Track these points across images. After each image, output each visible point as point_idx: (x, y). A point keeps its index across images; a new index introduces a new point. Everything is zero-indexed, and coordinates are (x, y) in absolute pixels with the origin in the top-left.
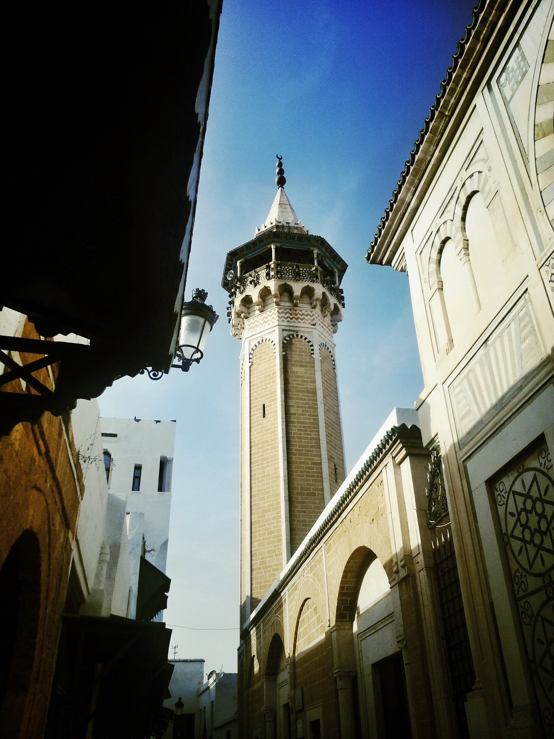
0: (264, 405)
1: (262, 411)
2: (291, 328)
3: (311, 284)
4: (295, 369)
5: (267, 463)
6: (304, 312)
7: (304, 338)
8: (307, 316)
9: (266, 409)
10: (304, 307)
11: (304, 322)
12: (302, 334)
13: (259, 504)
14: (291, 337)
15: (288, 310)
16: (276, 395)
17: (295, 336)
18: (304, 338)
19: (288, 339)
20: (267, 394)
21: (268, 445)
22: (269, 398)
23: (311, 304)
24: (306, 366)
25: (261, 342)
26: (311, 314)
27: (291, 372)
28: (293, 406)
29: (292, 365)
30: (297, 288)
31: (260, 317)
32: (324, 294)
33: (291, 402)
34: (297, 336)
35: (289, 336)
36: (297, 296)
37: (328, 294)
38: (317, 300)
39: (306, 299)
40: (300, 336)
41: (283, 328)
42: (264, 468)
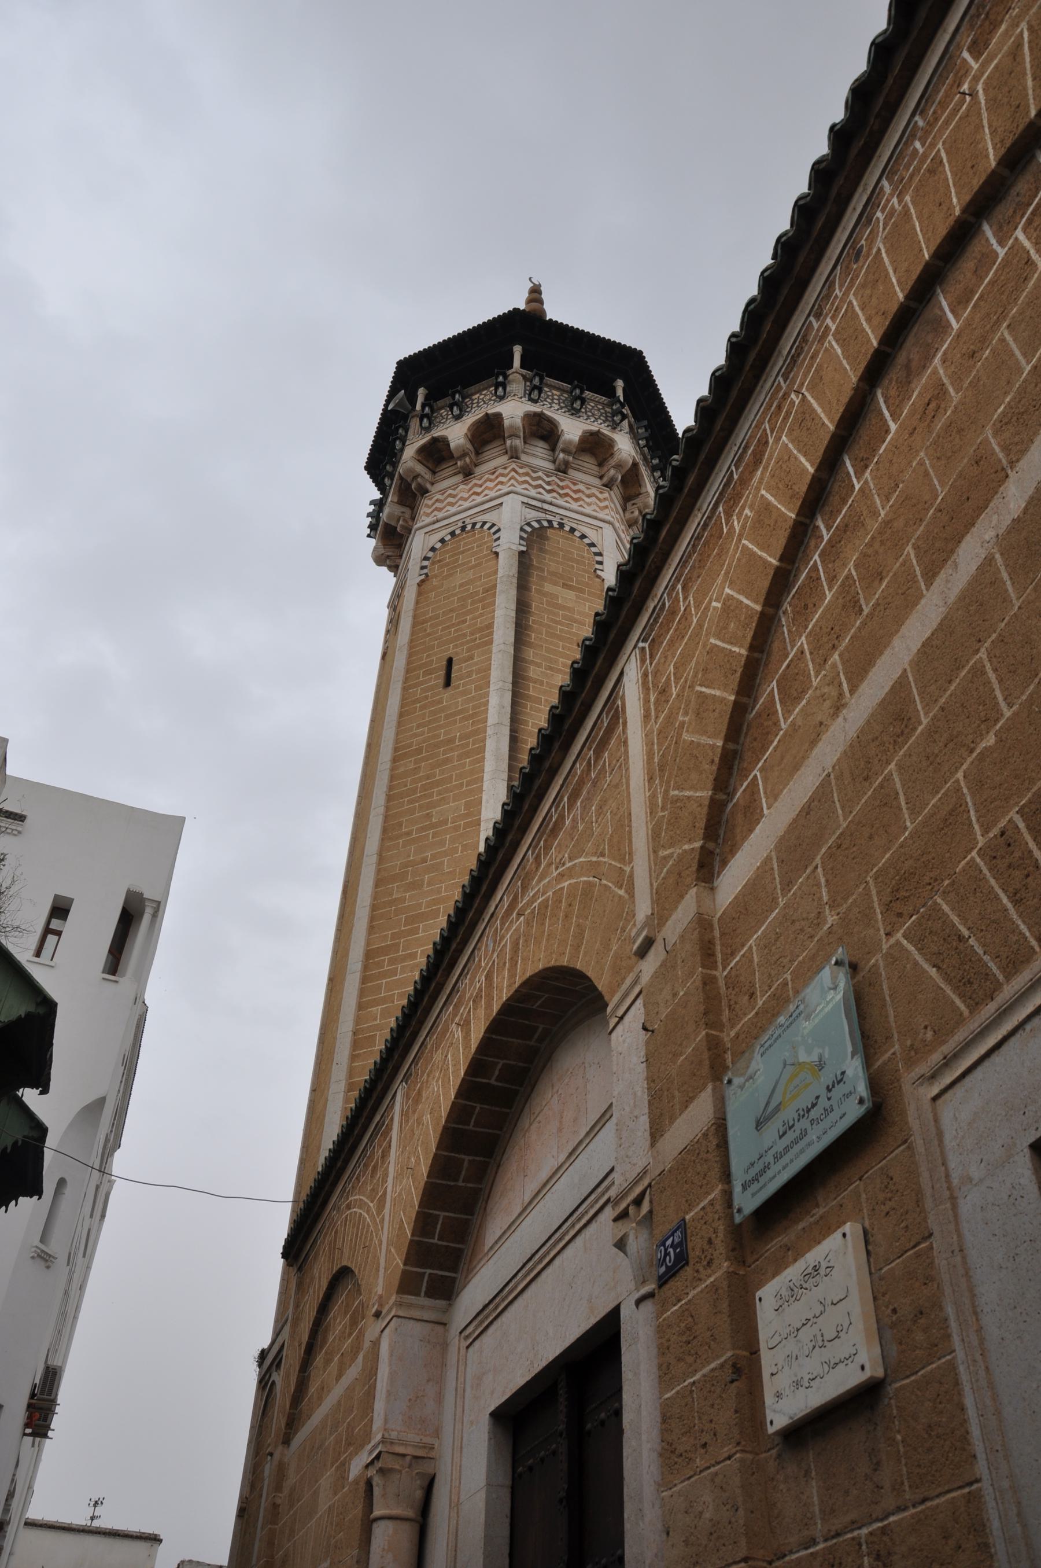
0: (450, 661)
1: (443, 673)
2: (546, 506)
3: (606, 431)
4: (548, 587)
5: (439, 793)
6: (581, 487)
7: (577, 534)
8: (589, 496)
9: (455, 668)
10: (585, 477)
11: (581, 506)
12: (574, 526)
13: (403, 900)
14: (545, 524)
15: (540, 474)
16: (492, 633)
17: (555, 525)
18: (577, 534)
19: (536, 525)
20: (465, 635)
21: (452, 750)
22: (468, 642)
23: (601, 478)
24: (582, 591)
25: (458, 532)
26: (600, 496)
27: (538, 591)
28: (539, 665)
29: (543, 579)
30: (573, 429)
31: (462, 487)
32: (635, 465)
33: (530, 654)
34: (561, 525)
35: (539, 521)
36: (570, 442)
37: (644, 471)
38: (618, 466)
39: (589, 462)
40: (567, 528)
41: (526, 500)
42: (431, 805)
